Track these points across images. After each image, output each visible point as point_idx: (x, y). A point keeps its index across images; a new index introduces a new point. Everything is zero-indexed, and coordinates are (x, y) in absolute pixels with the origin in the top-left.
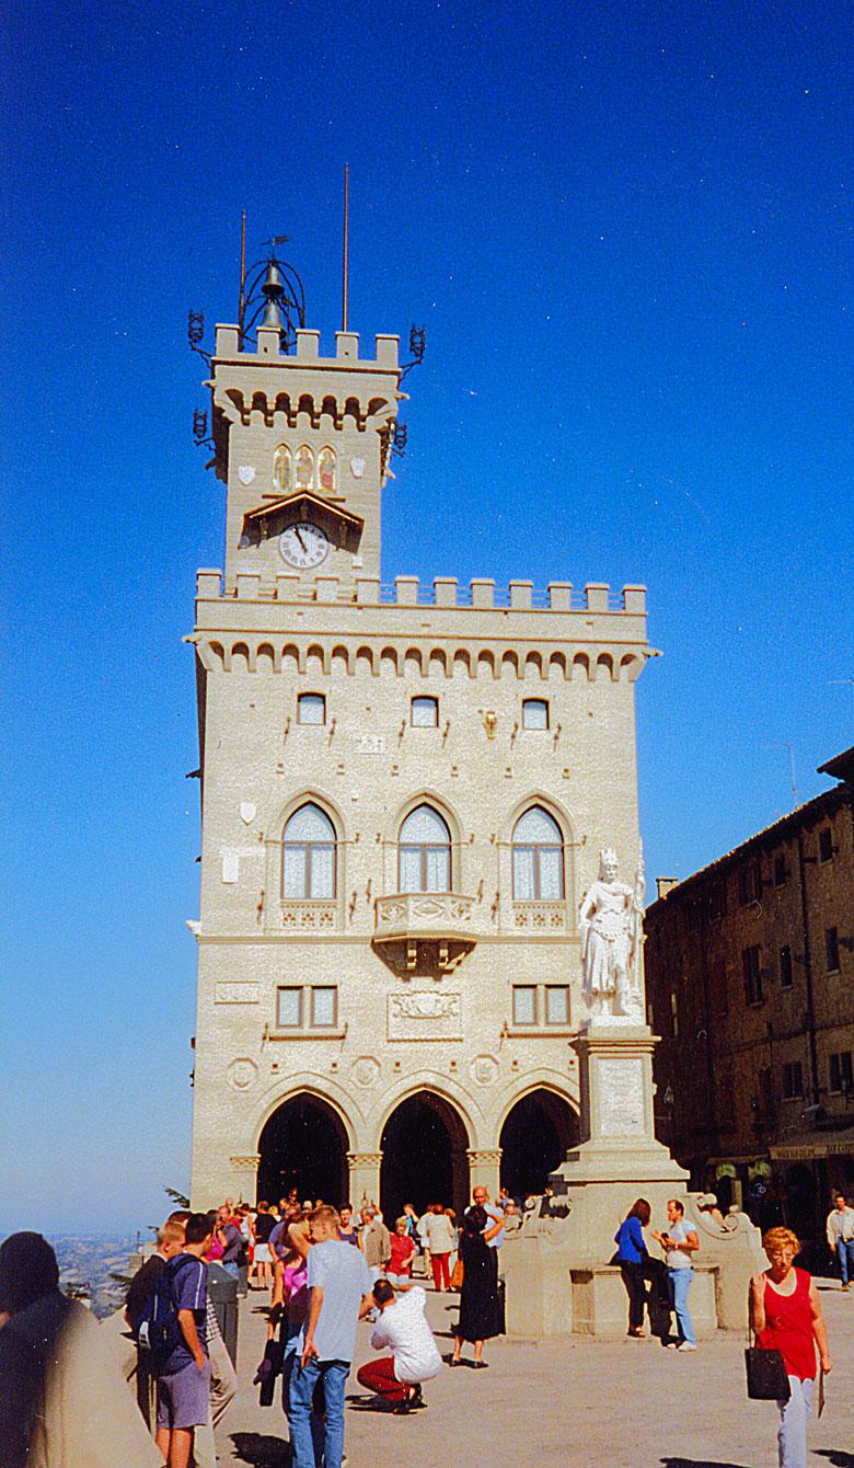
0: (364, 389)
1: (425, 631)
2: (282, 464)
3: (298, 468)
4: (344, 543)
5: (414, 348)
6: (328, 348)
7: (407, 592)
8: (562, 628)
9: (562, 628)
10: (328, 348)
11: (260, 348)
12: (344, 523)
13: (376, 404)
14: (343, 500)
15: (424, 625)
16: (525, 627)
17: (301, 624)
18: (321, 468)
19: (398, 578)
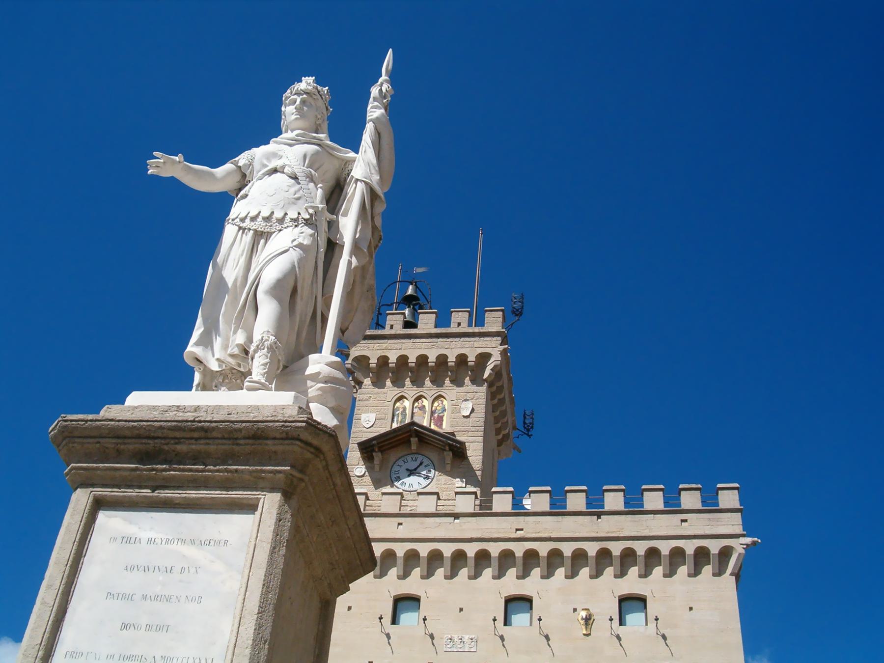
0: (471, 349)
1: (520, 534)
2: (401, 410)
3: (413, 413)
4: (448, 467)
5: (514, 314)
6: (443, 320)
7: (502, 502)
8: (657, 526)
9: (657, 526)
10: (443, 320)
11: (388, 327)
12: (447, 448)
13: (484, 358)
14: (453, 434)
15: (517, 530)
16: (618, 527)
17: (401, 533)
18: (432, 413)
19: (494, 489)
